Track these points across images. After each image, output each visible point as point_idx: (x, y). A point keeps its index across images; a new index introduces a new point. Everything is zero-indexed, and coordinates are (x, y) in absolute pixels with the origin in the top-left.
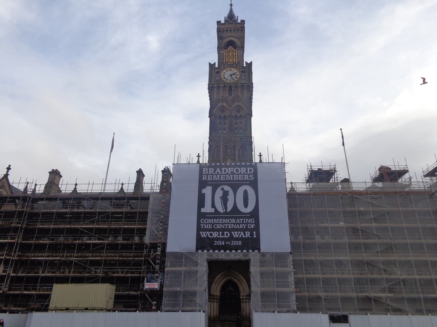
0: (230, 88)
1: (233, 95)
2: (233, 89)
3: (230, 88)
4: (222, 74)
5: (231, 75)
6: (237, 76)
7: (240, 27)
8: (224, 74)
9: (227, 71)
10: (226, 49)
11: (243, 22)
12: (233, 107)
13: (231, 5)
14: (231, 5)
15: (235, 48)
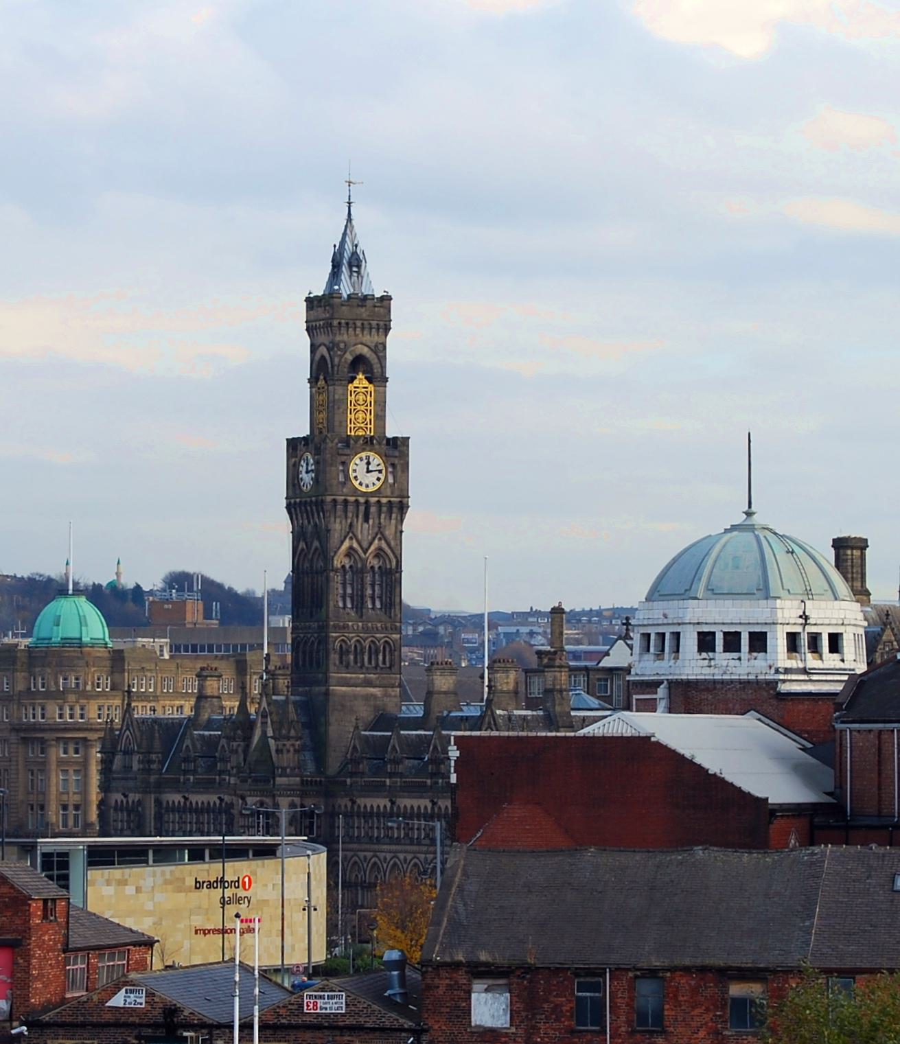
0: (367, 502)
1: (371, 522)
2: (373, 509)
3: (365, 507)
4: (352, 466)
5: (368, 471)
6: (380, 475)
7: (377, 313)
8: (355, 467)
9: (361, 459)
10: (352, 380)
11: (386, 300)
12: (370, 551)
13: (349, 203)
14: (349, 203)
15: (370, 382)
